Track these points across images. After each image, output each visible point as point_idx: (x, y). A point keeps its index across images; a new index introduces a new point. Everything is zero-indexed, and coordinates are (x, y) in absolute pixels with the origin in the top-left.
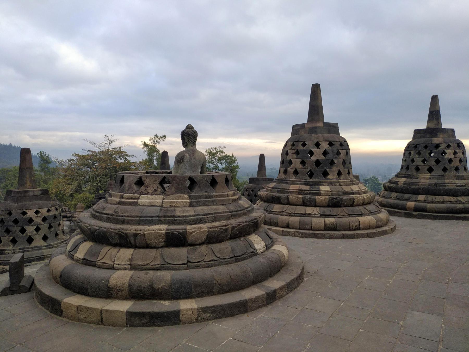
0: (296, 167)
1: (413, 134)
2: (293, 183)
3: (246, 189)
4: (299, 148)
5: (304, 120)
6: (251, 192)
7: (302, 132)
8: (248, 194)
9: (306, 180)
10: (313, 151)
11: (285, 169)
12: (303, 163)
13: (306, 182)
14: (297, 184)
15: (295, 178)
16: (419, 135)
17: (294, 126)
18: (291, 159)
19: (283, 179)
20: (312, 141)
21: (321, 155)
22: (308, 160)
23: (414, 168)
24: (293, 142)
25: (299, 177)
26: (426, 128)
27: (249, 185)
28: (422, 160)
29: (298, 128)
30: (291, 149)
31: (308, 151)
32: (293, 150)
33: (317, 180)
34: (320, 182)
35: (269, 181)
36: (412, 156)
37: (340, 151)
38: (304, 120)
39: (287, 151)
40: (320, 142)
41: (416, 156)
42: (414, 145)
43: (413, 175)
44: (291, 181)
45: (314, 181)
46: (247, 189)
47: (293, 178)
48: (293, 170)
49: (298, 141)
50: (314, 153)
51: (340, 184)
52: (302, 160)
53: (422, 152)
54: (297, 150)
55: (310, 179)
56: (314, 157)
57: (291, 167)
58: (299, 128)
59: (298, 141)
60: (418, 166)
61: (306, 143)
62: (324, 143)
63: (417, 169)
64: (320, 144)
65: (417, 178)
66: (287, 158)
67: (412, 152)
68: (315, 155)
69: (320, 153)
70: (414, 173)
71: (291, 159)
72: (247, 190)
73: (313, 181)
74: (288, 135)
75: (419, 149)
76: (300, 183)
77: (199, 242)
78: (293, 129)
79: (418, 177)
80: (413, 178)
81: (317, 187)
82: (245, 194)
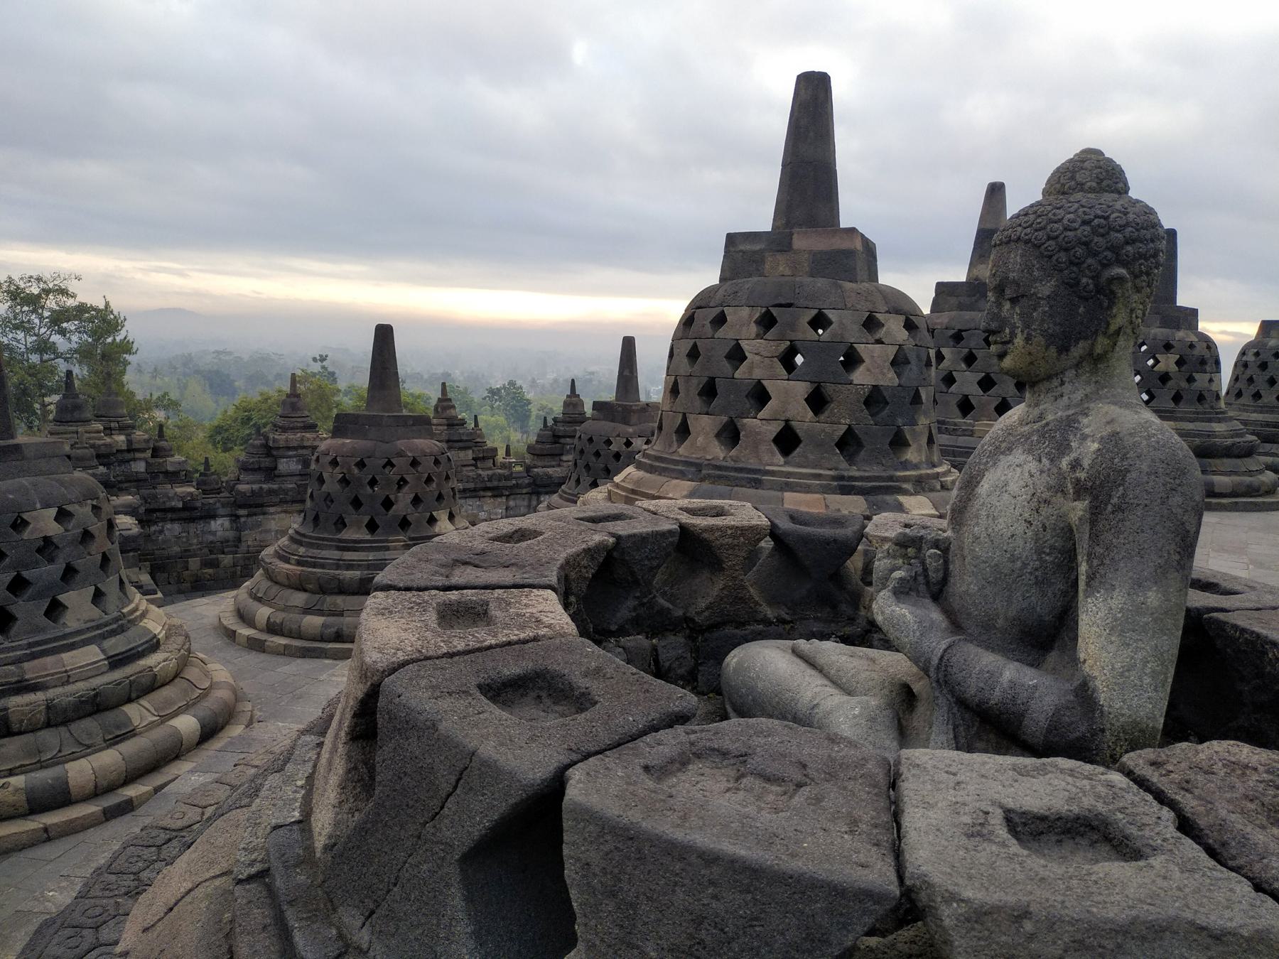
0: (789, 415)
1: (934, 295)
2: (787, 484)
3: (329, 459)
4: (800, 336)
5: (761, 218)
6: (356, 471)
7: (781, 269)
8: (344, 477)
9: (836, 469)
10: (859, 350)
11: (725, 419)
12: (817, 401)
13: (842, 478)
14: (807, 489)
15: (786, 463)
16: (953, 301)
17: (732, 239)
18: (763, 382)
19: (724, 464)
20: (849, 309)
21: (885, 371)
22: (840, 386)
23: (954, 401)
24: (764, 310)
25: (806, 457)
26: (965, 280)
27: (340, 441)
28: (979, 378)
29: (757, 247)
30: (758, 336)
31: (843, 348)
32: (772, 343)
33: (876, 471)
34: (891, 478)
35: (414, 428)
36: (945, 364)
37: (860, 348)
38: (761, 218)
39: (733, 343)
40: (878, 315)
41: (960, 365)
42: (952, 332)
43: (955, 424)
44: (772, 473)
45: (867, 474)
46: (335, 458)
47: (776, 462)
48: (774, 428)
49: (790, 305)
50: (863, 361)
51: (941, 482)
52: (816, 385)
53: (979, 354)
54: (791, 341)
55: (848, 467)
56: (860, 376)
57: (760, 415)
58: (761, 251)
59: (790, 305)
60: (966, 396)
61: (831, 314)
62: (891, 320)
63: (966, 406)
64: (883, 325)
65: (971, 433)
66: (736, 375)
67: (945, 351)
68: (868, 370)
69: (885, 361)
70: (957, 417)
71: (759, 382)
72: (334, 463)
73: (862, 474)
74: (710, 276)
75: (972, 344)
76: (821, 486)
77: (168, 680)
78: (732, 249)
79: (972, 431)
80: (959, 433)
81: (888, 498)
82: (325, 475)
